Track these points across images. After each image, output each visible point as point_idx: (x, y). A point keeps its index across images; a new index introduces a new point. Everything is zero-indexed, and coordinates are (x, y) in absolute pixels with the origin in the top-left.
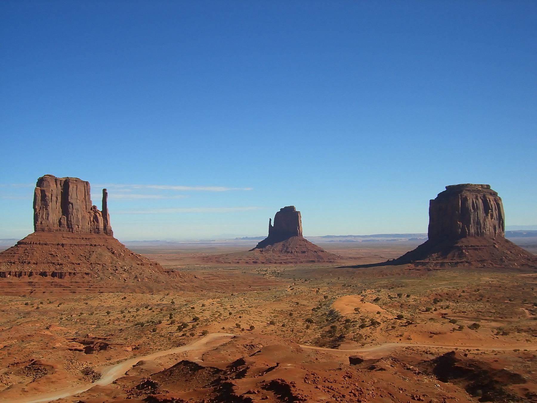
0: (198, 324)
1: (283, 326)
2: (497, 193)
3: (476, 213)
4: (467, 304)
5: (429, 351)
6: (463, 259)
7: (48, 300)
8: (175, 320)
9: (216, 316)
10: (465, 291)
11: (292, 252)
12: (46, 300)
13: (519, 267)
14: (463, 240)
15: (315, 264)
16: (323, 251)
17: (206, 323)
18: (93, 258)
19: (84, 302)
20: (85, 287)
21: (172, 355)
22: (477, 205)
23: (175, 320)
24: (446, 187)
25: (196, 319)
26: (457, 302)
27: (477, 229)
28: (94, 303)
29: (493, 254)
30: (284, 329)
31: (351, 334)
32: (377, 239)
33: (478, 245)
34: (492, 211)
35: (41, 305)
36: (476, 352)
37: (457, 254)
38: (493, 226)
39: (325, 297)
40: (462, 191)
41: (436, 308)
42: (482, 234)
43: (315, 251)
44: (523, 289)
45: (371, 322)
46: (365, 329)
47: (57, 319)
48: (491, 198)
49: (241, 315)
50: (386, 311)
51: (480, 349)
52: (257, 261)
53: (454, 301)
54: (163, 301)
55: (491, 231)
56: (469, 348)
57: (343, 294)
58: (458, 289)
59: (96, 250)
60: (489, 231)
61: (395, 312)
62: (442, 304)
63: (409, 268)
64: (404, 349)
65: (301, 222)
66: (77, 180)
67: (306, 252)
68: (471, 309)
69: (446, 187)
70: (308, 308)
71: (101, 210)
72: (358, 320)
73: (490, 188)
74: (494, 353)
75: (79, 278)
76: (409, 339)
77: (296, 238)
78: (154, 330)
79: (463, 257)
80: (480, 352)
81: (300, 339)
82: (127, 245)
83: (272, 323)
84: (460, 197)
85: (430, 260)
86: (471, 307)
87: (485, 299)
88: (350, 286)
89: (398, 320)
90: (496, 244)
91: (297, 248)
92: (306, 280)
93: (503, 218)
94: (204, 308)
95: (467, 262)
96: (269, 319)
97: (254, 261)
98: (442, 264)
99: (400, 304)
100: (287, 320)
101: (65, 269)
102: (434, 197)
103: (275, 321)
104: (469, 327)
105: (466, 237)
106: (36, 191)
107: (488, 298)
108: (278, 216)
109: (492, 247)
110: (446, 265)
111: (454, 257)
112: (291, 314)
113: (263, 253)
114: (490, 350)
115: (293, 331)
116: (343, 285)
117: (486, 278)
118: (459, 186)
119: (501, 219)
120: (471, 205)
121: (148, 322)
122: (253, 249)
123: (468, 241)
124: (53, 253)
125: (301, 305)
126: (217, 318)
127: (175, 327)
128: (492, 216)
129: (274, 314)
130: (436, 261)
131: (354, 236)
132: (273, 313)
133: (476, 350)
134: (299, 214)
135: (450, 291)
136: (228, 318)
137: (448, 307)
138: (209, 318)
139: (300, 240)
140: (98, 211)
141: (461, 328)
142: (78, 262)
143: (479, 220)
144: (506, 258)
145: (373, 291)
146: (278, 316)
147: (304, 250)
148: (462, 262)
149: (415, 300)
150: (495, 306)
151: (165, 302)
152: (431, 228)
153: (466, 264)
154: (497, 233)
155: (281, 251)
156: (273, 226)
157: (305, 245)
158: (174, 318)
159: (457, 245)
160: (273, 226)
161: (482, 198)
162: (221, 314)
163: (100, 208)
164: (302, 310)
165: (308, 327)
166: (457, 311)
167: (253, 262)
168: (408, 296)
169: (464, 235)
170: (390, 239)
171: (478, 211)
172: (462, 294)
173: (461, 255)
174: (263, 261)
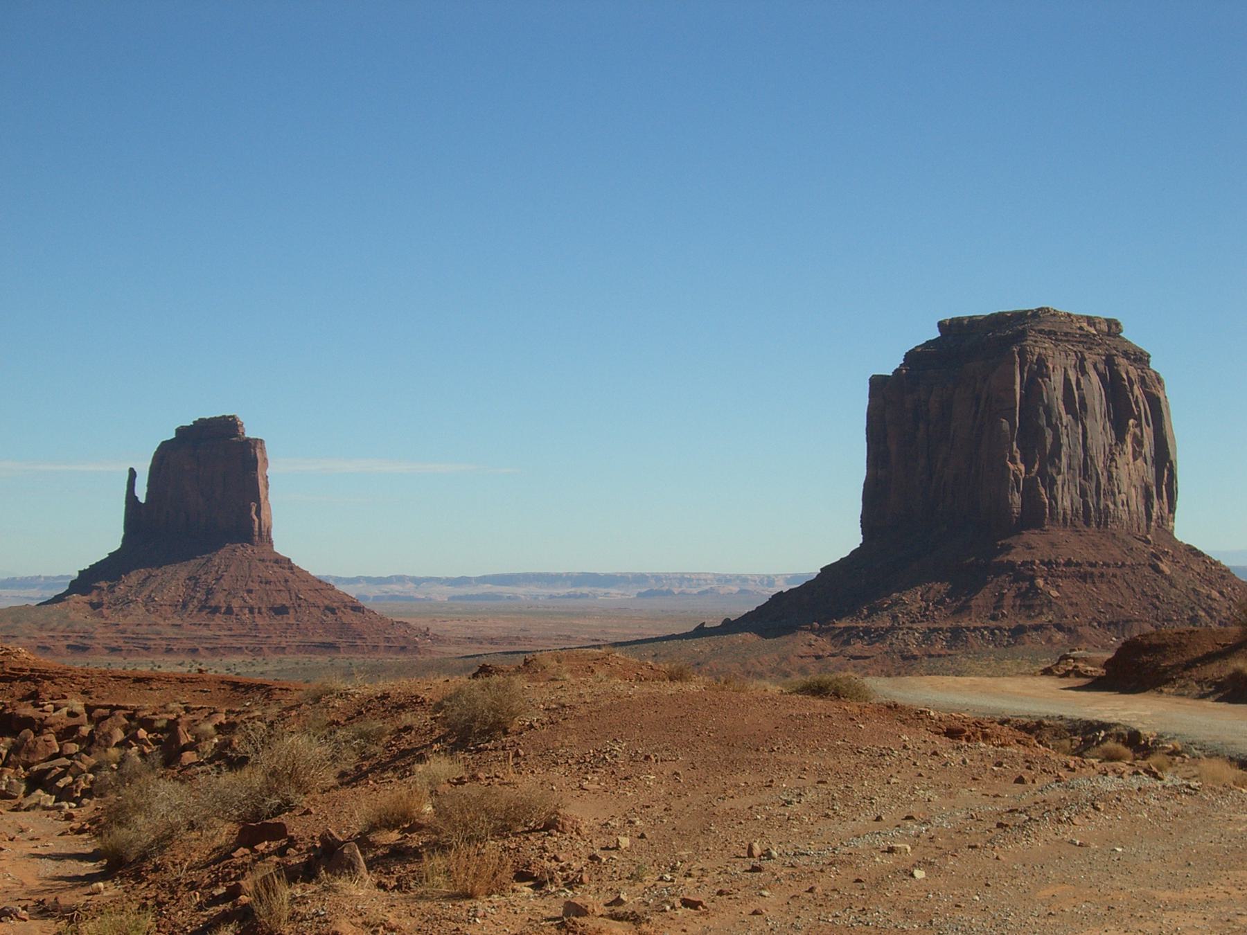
2: (1149, 356)
3: (1080, 431)
6: (1041, 613)
11: (229, 611)
14: (1031, 536)
15: (341, 656)
16: (357, 608)
22: (1082, 399)
24: (941, 325)
27: (1083, 494)
29: (1158, 598)
32: (506, 590)
34: (1139, 425)
37: (1012, 593)
38: (1141, 486)
40: (1022, 335)
42: (1104, 517)
43: (327, 608)
48: (1126, 368)
52: (86, 641)
55: (1133, 508)
60: (1126, 508)
63: (811, 651)
65: (267, 487)
67: (291, 611)
69: (941, 325)
73: (1121, 334)
77: (244, 551)
79: (1041, 605)
84: (1017, 359)
85: (895, 618)
90: (1159, 559)
91: (250, 591)
93: (1172, 457)
95: (1060, 628)
97: (70, 642)
98: (956, 635)
102: (889, 364)
105: (1044, 526)
108: (165, 457)
109: (1147, 571)
110: (971, 640)
111: (998, 607)
113: (105, 612)
118: (998, 320)
120: (1059, 394)
122: (58, 599)
123: (1053, 545)
128: (1138, 442)
130: (925, 625)
131: (418, 581)
134: (258, 451)
139: (263, 561)
143: (1091, 459)
144: (1212, 617)
147: (282, 599)
148: (1037, 628)
154: (1154, 516)
155: (185, 606)
156: (142, 499)
157: (286, 581)
159: (1010, 558)
160: (142, 499)
161: (1101, 367)
167: (69, 646)
169: (1034, 516)
170: (563, 591)
171: (1088, 424)
173: (1029, 598)
174: (114, 645)
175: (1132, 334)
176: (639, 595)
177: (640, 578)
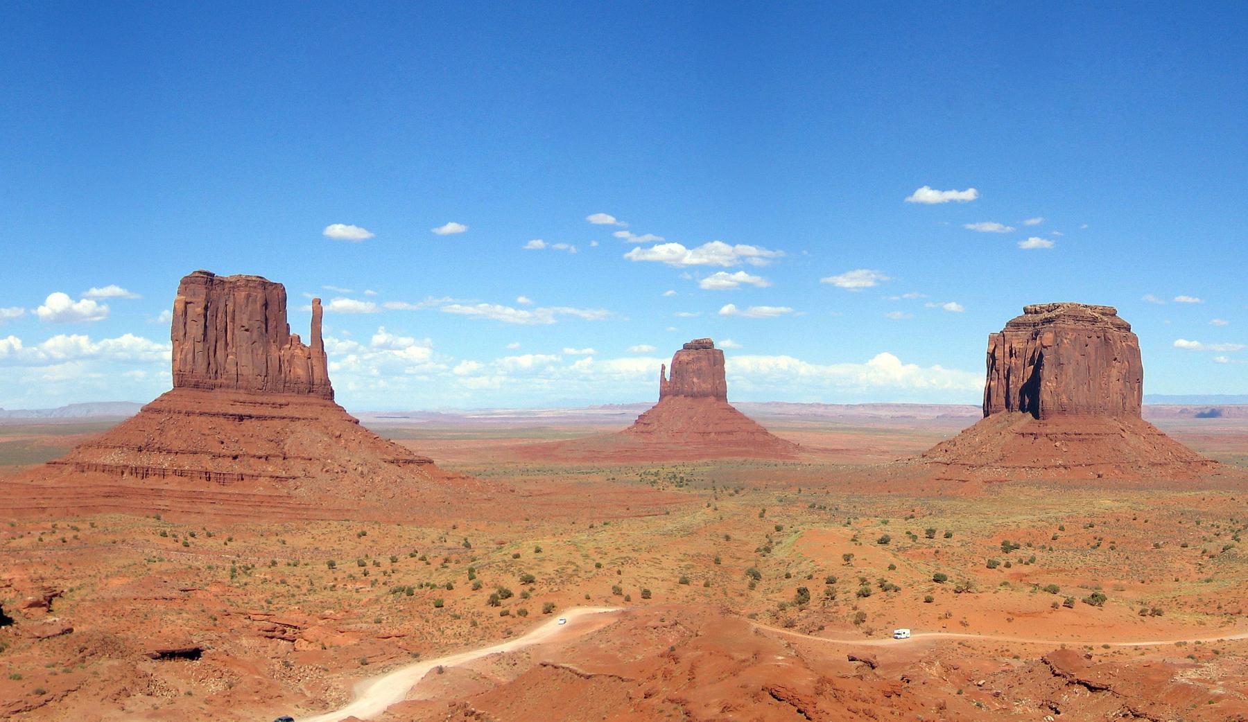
4: (1070, 554)
5: (1007, 651)
7: (204, 529)
10: (1065, 528)
12: (200, 529)
13: (1169, 479)
18: (289, 446)
19: (278, 537)
20: (275, 507)
24: (1025, 309)
26: (1051, 549)
28: (300, 541)
31: (845, 611)
33: (1088, 432)
35: (193, 539)
36: (1104, 651)
41: (1008, 562)
44: (1180, 522)
47: (224, 569)
51: (1109, 644)
56: (1089, 644)
58: (1051, 524)
59: (299, 430)
62: (1019, 553)
64: (956, 645)
66: (264, 284)
71: (308, 344)
74: (1138, 652)
75: (262, 487)
76: (964, 624)
80: (1110, 651)
82: (362, 420)
87: (1105, 546)
101: (237, 468)
102: (999, 327)
106: (177, 307)
107: (1114, 543)
114: (1131, 647)
117: (1105, 502)
119: (1135, 377)
124: (207, 432)
135: (1033, 526)
136: (594, 575)
137: (1032, 560)
140: (305, 346)
141: (1069, 604)
142: (260, 453)
150: (1127, 558)
153: (1063, 471)
163: (306, 340)
170: (899, 414)
172: (1059, 533)
175: (1123, 315)
176: (938, 417)
177: (940, 407)
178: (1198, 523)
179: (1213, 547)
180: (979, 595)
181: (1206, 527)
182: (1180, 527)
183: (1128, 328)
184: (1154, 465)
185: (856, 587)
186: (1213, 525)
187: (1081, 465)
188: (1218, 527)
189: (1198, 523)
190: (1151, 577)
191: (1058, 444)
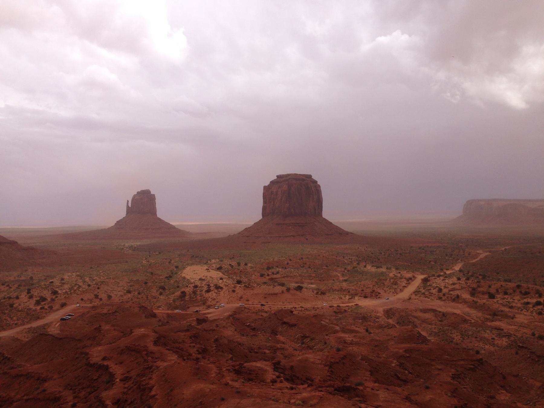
0: (57, 297)
1: (139, 294)
8: (33, 294)
9: (75, 288)
10: (292, 259)
17: (65, 296)
21: (29, 328)
23: (33, 294)
24: (277, 176)
25: (55, 293)
26: (286, 268)
30: (140, 296)
39: (177, 267)
45: (215, 287)
46: (211, 293)
49: (100, 287)
50: (228, 277)
53: (283, 268)
54: (21, 277)
57: (192, 264)
58: (286, 258)
61: (235, 277)
62: (273, 270)
68: (297, 274)
69: (277, 176)
70: (161, 277)
72: (204, 286)
78: (11, 306)
81: (154, 304)
83: (129, 292)
86: (296, 272)
88: (198, 257)
89: (237, 285)
90: (315, 222)
92: (160, 253)
94: (63, 281)
95: (294, 236)
96: (125, 288)
99: (239, 272)
100: (142, 289)
102: (267, 183)
103: (131, 290)
104: (295, 289)
112: (146, 283)
115: (147, 297)
116: (191, 256)
121: (4, 298)
125: (155, 274)
126: (75, 291)
127: (33, 301)
129: (131, 284)
132: (129, 283)
133: (301, 307)
137: (278, 273)
138: (68, 291)
145: (216, 261)
146: (134, 285)
149: (252, 268)
150: (315, 271)
151: (23, 278)
152: (264, 209)
156: (130, 206)
158: (32, 293)
160: (130, 206)
162: (80, 287)
164: (156, 279)
165: (161, 294)
166: (285, 275)
168: (246, 264)
178: (344, 257)
179: (349, 268)
180: (253, 288)
181: (347, 259)
182: (337, 259)
183: (316, 182)
184: (327, 235)
185: (205, 288)
186: (349, 258)
187: (299, 235)
188: (352, 259)
189: (344, 257)
190: (324, 279)
191: (290, 227)
